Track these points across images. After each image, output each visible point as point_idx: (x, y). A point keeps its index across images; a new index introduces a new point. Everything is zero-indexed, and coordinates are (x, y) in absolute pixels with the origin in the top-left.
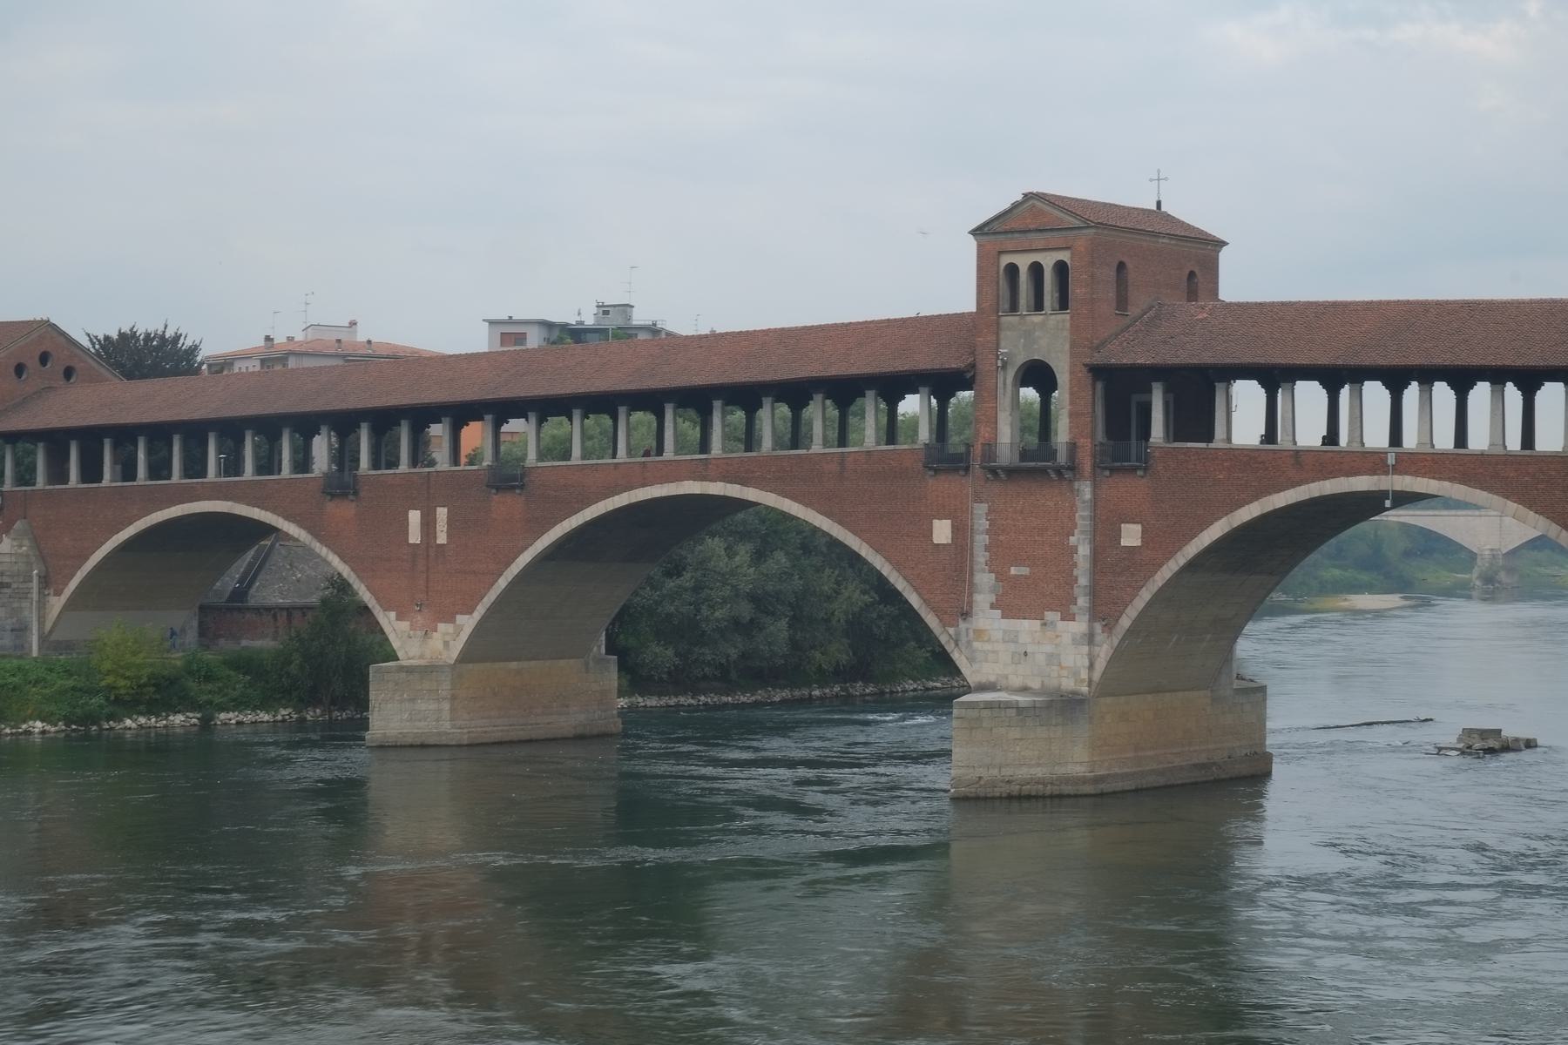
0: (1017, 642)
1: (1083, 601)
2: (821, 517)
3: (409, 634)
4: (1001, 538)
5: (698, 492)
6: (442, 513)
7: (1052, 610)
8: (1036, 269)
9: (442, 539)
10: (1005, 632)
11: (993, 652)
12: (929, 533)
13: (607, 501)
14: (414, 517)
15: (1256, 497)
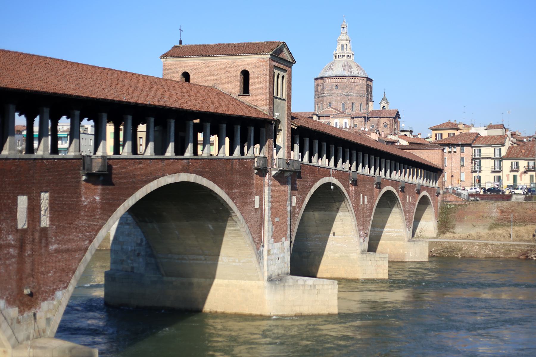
1: (289, 232)
2: (227, 196)
3: (18, 319)
5: (186, 180)
6: (45, 197)
7: (284, 237)
8: (279, 75)
9: (45, 222)
13: (147, 186)
14: (23, 201)
15: (313, 185)
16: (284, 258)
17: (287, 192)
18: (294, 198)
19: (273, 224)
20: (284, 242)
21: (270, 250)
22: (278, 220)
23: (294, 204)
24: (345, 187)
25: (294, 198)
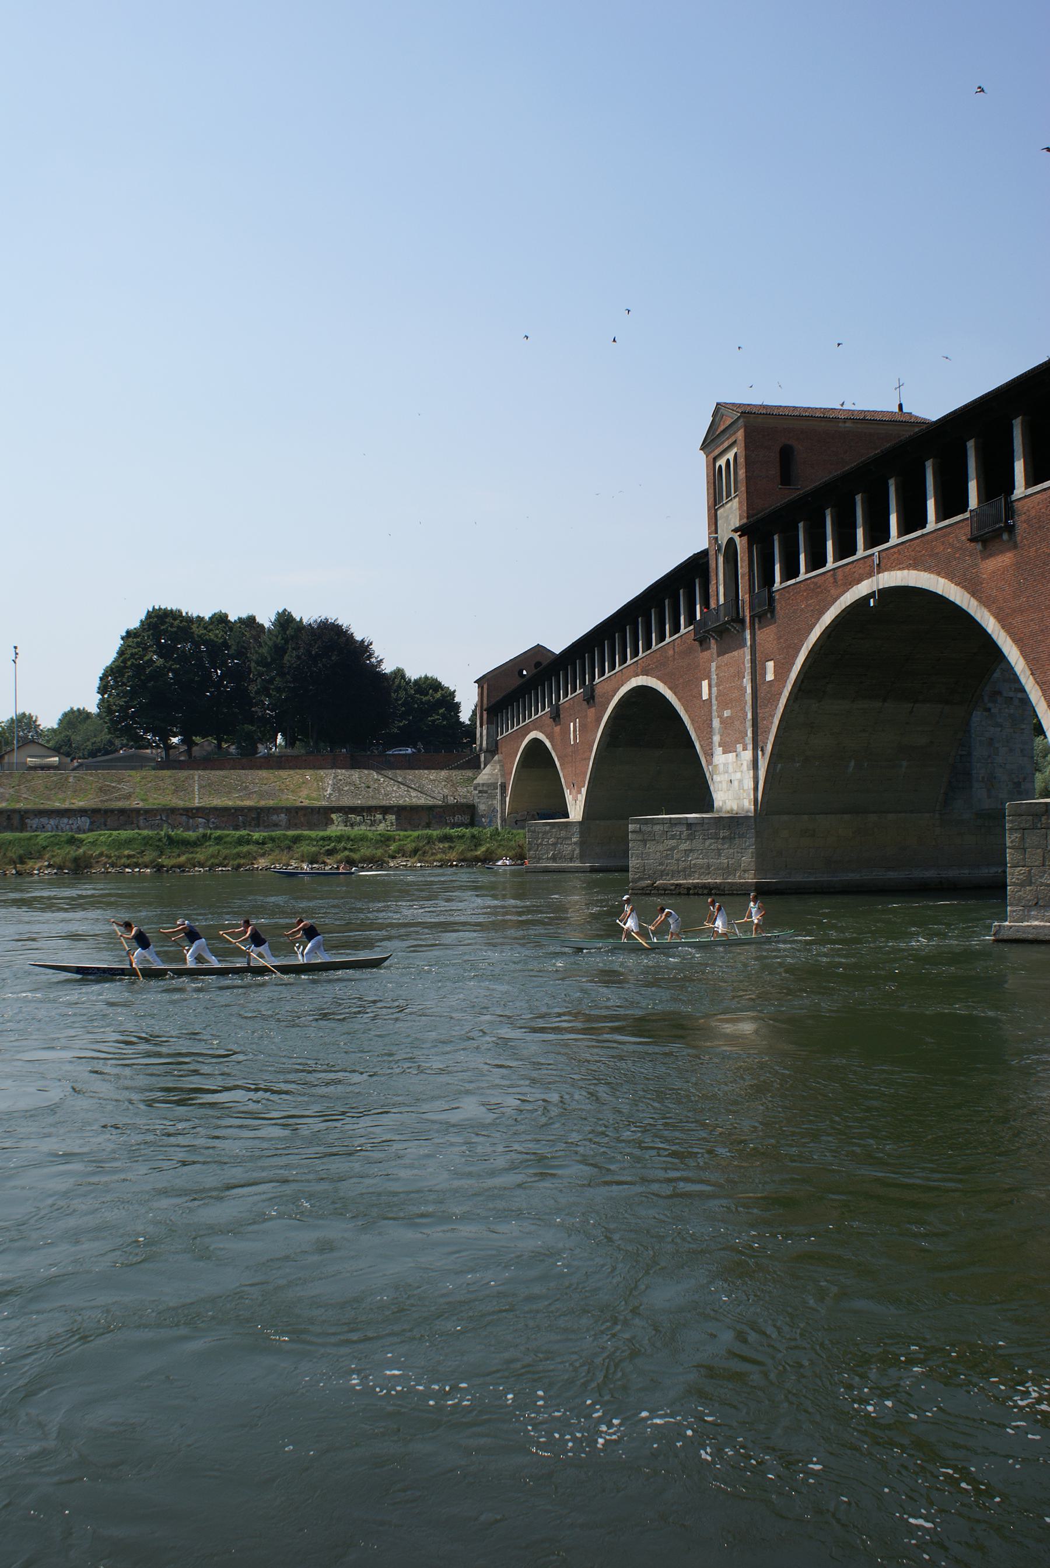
0: (727, 772)
4: (721, 688)
10: (724, 764)
11: (721, 782)
12: (701, 695)
14: (572, 724)
16: (740, 781)
17: (745, 657)
18: (770, 665)
19: (721, 723)
20: (740, 752)
21: (717, 765)
22: (729, 715)
23: (770, 676)
24: (950, 577)
25: (770, 665)
